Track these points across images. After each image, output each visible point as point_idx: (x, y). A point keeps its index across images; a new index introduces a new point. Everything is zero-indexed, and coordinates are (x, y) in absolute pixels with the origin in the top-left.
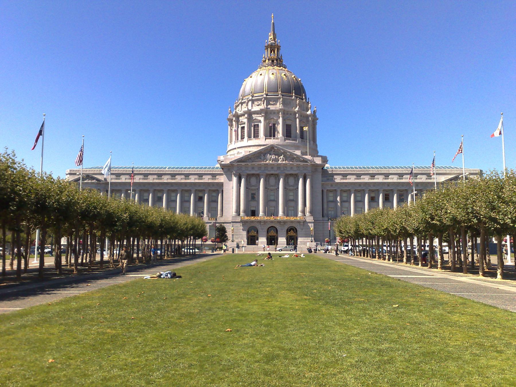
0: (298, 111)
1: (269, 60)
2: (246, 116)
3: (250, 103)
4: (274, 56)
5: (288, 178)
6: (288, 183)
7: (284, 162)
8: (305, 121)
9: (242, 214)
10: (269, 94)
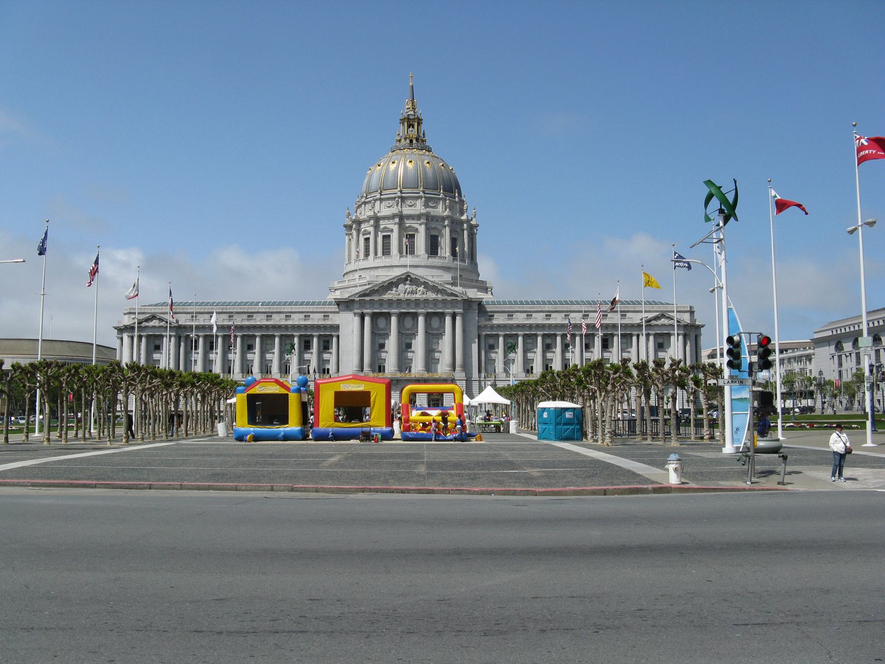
0: (448, 217)
1: (405, 139)
2: (372, 222)
3: (378, 202)
4: (413, 132)
5: (431, 318)
7: (424, 296)
8: (458, 230)
9: (366, 368)
10: (405, 191)
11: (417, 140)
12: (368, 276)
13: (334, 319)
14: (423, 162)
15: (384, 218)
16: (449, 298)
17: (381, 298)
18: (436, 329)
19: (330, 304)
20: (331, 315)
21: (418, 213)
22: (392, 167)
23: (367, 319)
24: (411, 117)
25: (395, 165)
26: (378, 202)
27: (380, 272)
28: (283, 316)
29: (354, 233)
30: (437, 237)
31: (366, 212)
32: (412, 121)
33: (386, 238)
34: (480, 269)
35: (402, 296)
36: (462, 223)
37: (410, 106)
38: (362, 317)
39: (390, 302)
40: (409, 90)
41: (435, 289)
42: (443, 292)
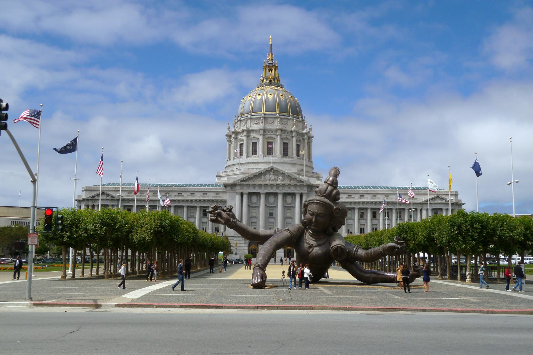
0: (295, 131)
1: (267, 79)
3: (249, 121)
4: (271, 75)
5: (286, 197)
6: (286, 201)
8: (301, 139)
11: (274, 80)
12: (243, 169)
13: (224, 197)
14: (278, 95)
15: (253, 131)
16: (299, 184)
17: (254, 183)
18: (289, 204)
19: (220, 186)
20: (221, 194)
21: (275, 128)
22: (259, 98)
23: (245, 197)
24: (271, 65)
25: (260, 97)
26: (249, 121)
27: (251, 166)
28: (189, 194)
29: (233, 140)
30: (287, 143)
31: (241, 127)
32: (270, 68)
33: (255, 144)
34: (314, 166)
35: (267, 182)
36: (303, 135)
37: (270, 57)
38: (242, 195)
39: (260, 186)
40: (269, 47)
41: (289, 177)
42: (295, 179)
